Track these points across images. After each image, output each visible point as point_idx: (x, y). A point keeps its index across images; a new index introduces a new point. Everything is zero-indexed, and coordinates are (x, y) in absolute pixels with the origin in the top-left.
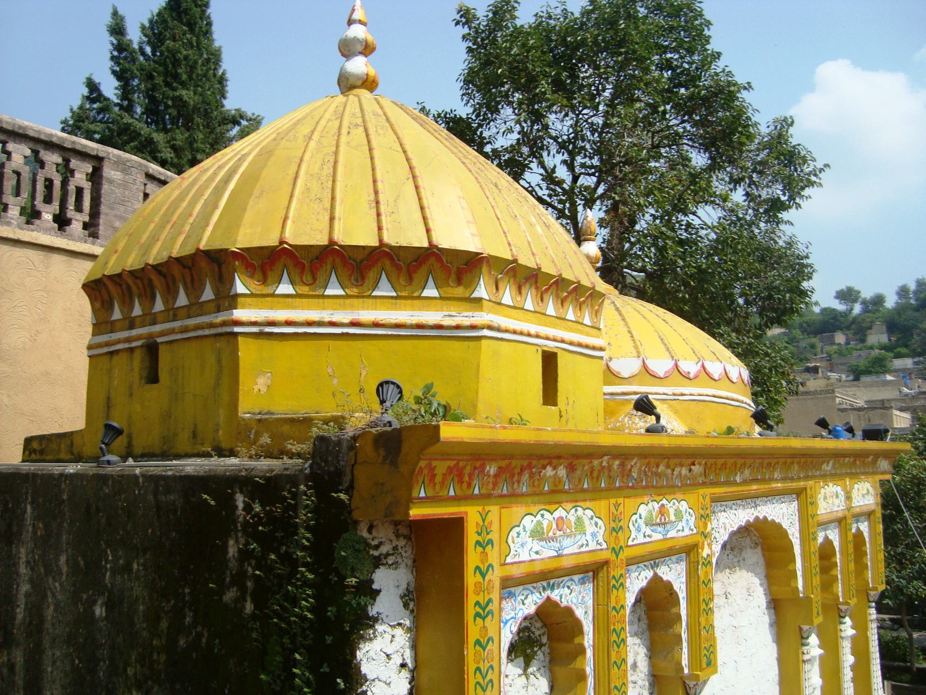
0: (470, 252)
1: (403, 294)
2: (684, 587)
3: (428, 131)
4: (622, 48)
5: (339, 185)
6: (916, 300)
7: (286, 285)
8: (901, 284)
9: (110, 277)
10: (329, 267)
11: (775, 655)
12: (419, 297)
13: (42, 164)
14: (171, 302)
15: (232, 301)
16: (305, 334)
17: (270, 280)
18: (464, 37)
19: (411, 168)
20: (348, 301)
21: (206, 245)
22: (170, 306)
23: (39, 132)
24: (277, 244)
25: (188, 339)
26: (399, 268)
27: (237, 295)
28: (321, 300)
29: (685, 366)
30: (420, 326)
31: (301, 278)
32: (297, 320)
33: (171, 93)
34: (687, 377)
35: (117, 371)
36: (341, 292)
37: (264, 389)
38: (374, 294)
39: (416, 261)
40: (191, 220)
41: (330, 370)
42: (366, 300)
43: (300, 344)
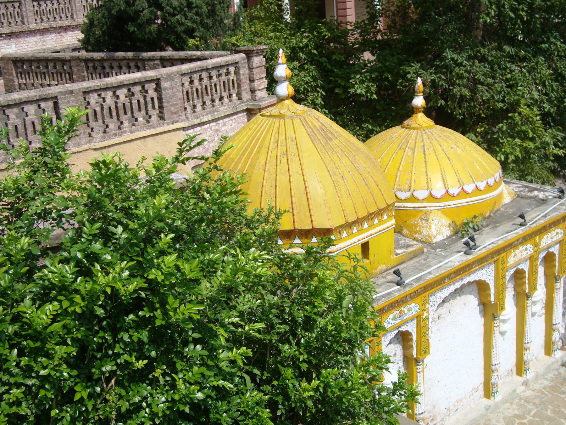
2: (415, 329)
3: (315, 146)
5: (278, 199)
11: (483, 323)
13: (133, 94)
19: (306, 187)
23: (129, 80)
26: (302, 235)
29: (451, 191)
34: (453, 196)
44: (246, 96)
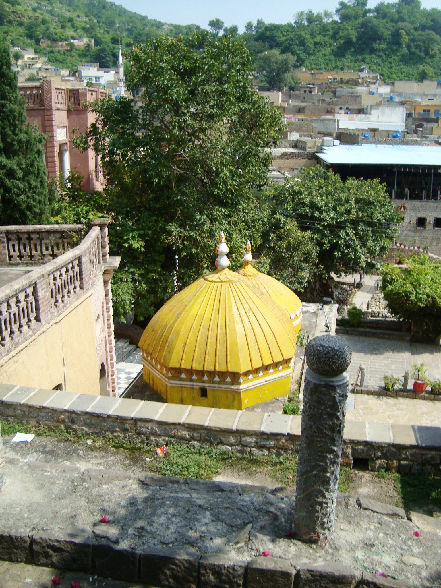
6: (257, 32)
8: (248, 21)
15: (239, 384)
33: (17, 138)
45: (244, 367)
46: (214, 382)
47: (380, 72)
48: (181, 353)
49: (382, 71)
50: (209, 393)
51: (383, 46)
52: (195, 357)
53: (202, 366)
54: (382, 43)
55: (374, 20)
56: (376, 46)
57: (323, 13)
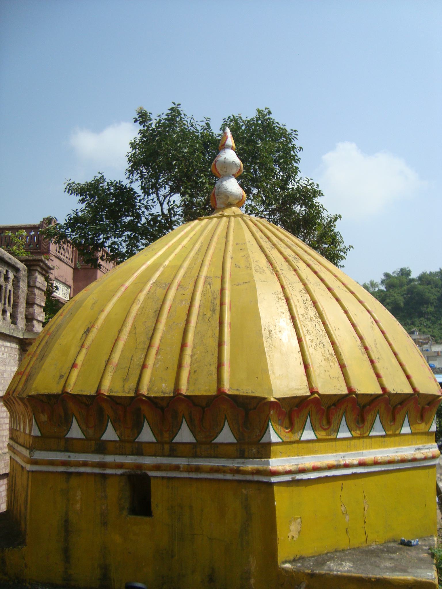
0: (435, 395)
1: (390, 433)
4: (257, 159)
7: (309, 432)
9: (75, 397)
10: (341, 411)
12: (400, 435)
14: (166, 435)
15: (265, 450)
16: (327, 477)
17: (296, 427)
18: (140, 131)
20: (353, 442)
21: (231, 388)
22: (167, 439)
24: (309, 394)
25: (197, 479)
27: (270, 444)
28: (334, 443)
30: (403, 461)
31: (320, 424)
32: (322, 466)
35: (79, 493)
36: (348, 435)
37: (296, 536)
38: (370, 435)
39: (401, 403)
40: (188, 351)
41: (343, 509)
42: (365, 440)
43: (321, 487)
44: (21, 323)
45: (285, 380)
46: (174, 450)
47: (431, 333)
48: (73, 351)
49: (433, 332)
50: (159, 496)
51: (431, 309)
52: (116, 357)
53: (132, 384)
54: (429, 306)
55: (419, 286)
56: (423, 309)
57: (369, 283)
